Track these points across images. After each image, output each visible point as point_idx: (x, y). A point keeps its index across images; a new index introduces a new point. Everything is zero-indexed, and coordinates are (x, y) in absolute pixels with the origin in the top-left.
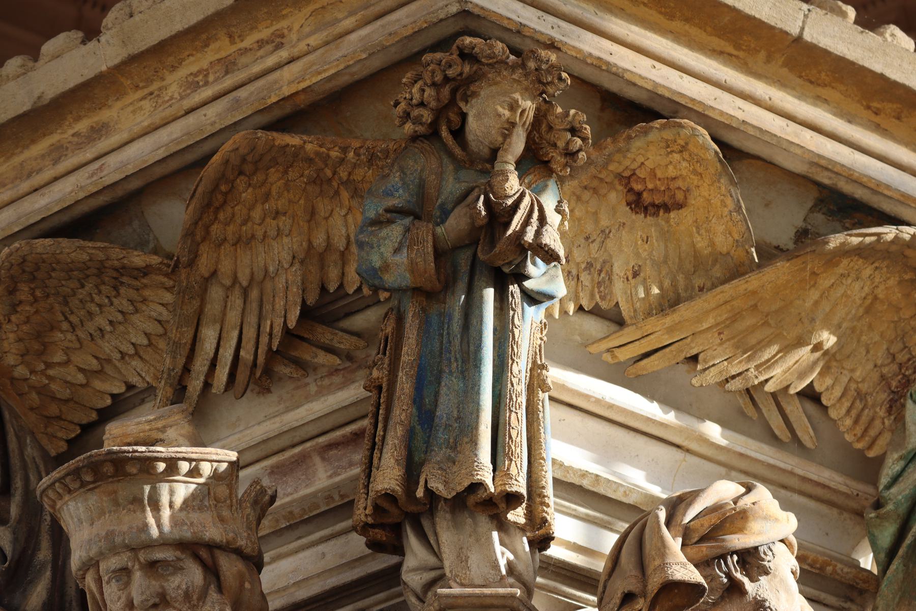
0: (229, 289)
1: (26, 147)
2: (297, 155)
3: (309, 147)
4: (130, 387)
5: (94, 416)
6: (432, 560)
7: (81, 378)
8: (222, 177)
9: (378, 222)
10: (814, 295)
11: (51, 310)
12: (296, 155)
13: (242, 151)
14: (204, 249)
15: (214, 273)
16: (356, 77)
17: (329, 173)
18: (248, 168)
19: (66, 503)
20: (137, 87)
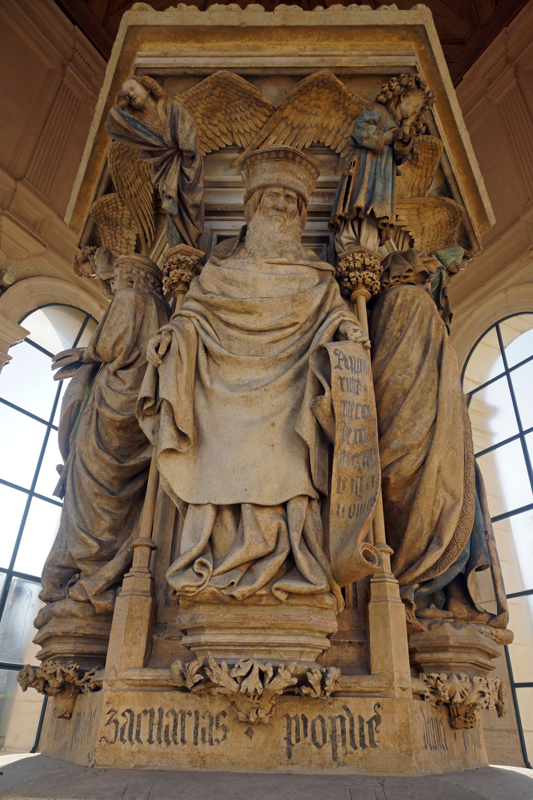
0: (287, 125)
1: (226, 41)
2: (338, 89)
3: (344, 88)
4: (235, 145)
5: (218, 149)
6: (354, 236)
7: (218, 134)
8: (311, 84)
9: (368, 122)
10: (431, 213)
11: (221, 103)
12: (337, 88)
13: (325, 77)
14: (289, 107)
15: (287, 117)
16: (366, 73)
17: (342, 101)
18: (321, 84)
19: (262, 163)
20: (277, 40)
